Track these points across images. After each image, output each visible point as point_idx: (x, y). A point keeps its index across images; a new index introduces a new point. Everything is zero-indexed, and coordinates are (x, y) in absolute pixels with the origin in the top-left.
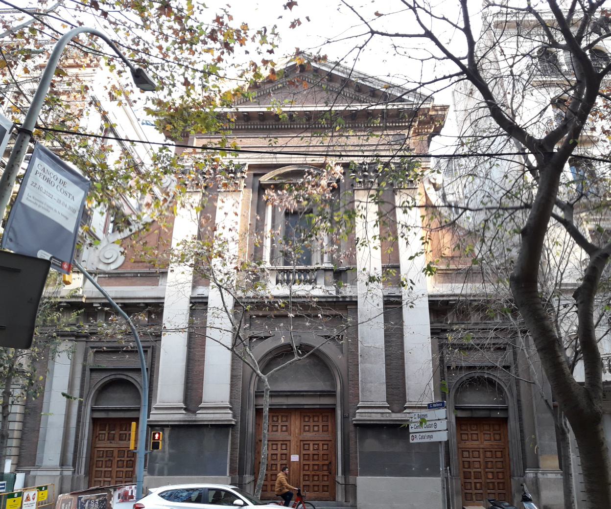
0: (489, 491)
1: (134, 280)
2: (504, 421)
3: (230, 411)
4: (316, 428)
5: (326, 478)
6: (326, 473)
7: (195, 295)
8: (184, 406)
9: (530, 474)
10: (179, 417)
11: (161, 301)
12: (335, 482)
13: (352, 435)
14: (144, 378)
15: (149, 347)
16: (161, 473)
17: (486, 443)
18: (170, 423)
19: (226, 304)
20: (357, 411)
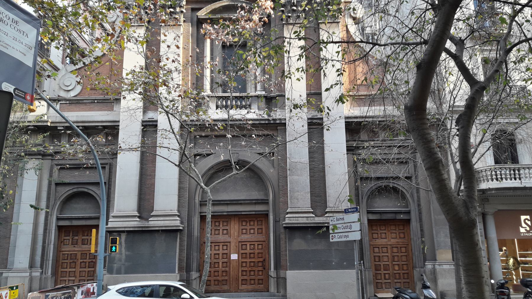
0: (396, 281)
1: (92, 105)
2: (408, 222)
3: (178, 218)
4: (252, 231)
5: (260, 273)
6: (260, 269)
7: (146, 119)
8: (138, 215)
9: (429, 266)
10: (134, 223)
11: (117, 124)
12: (268, 276)
13: (283, 236)
14: (103, 191)
15: (107, 164)
16: (119, 272)
17: (393, 240)
18: (126, 229)
19: (173, 127)
20: (286, 216)
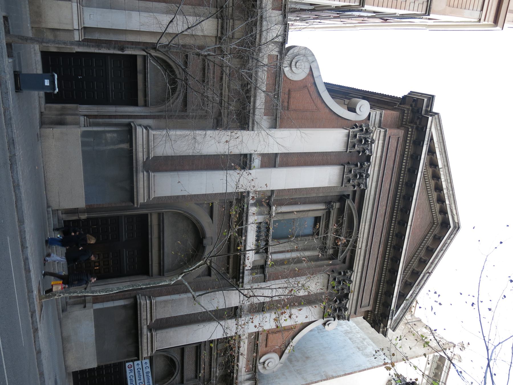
10: (141, 156)
11: (250, 128)
